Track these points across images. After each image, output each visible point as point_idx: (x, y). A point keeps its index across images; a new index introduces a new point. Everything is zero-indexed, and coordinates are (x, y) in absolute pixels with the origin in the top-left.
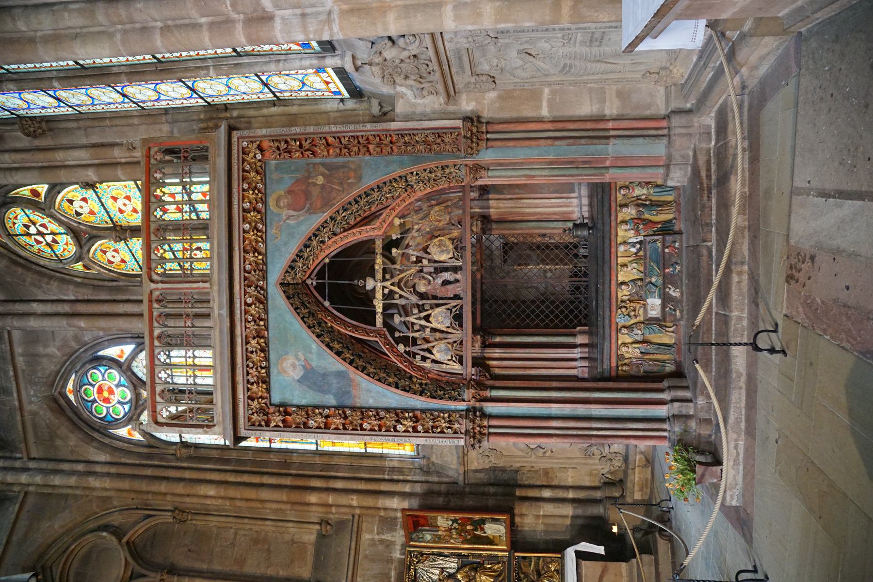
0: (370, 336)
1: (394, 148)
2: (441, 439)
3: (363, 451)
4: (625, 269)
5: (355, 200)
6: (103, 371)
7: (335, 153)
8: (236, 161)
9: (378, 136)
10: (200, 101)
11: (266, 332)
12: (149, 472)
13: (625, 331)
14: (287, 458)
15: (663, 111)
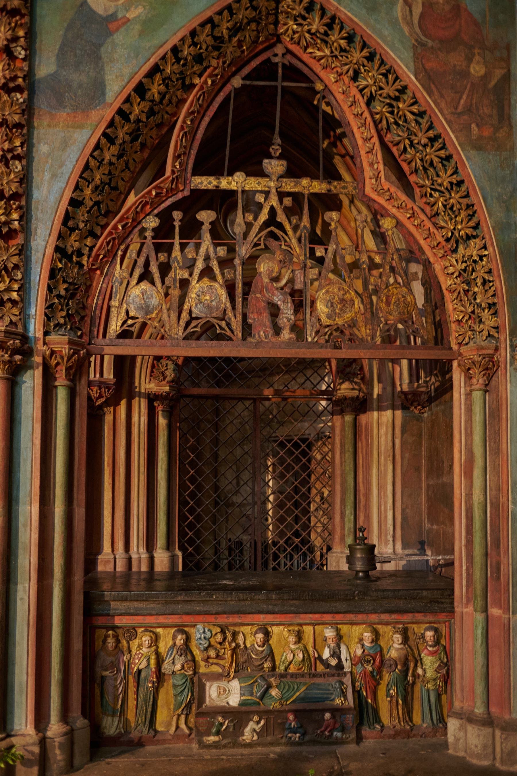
0: (174, 161)
4: (292, 639)
13: (180, 640)
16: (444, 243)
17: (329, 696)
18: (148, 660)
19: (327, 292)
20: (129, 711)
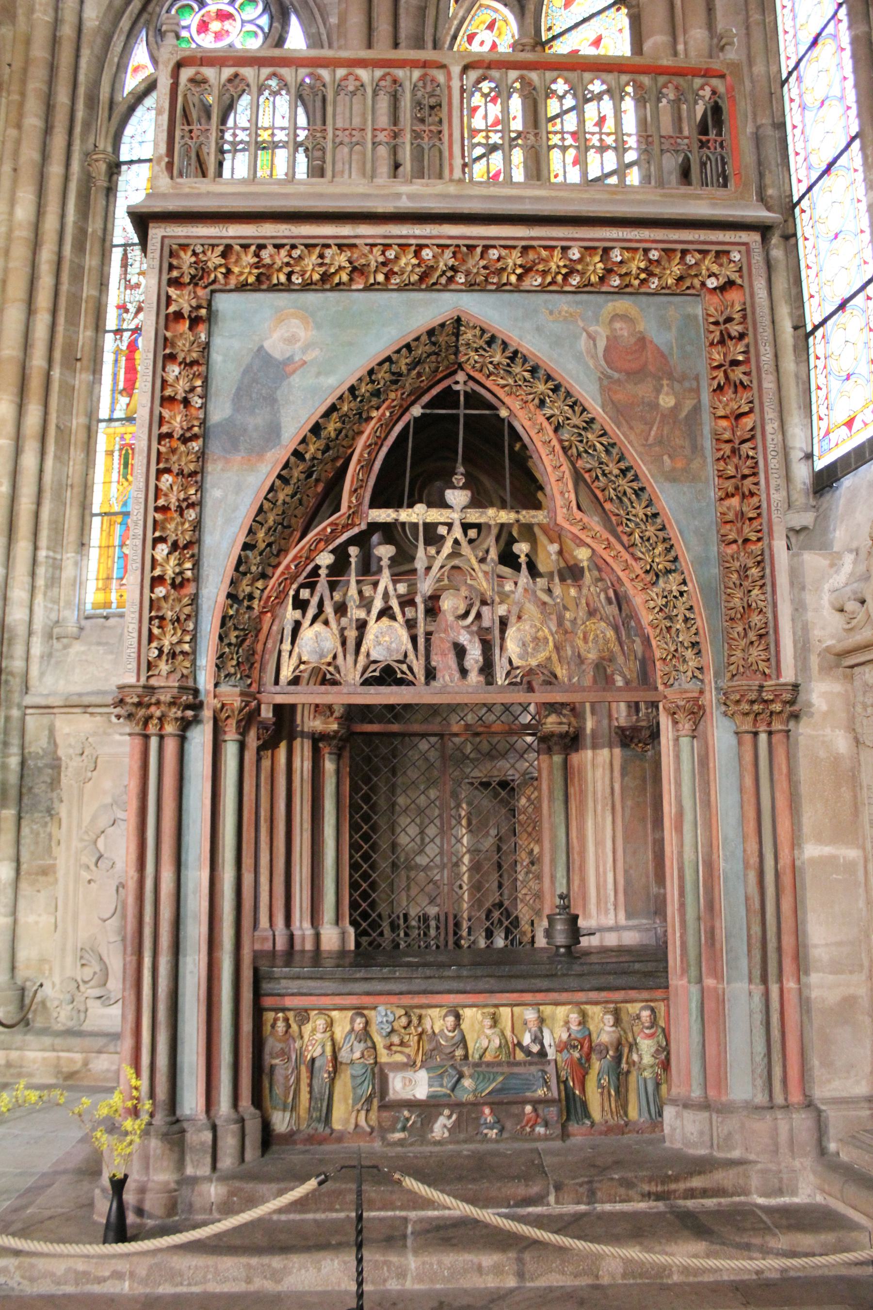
1: (734, 546)
2: (136, 635)
3: (96, 509)
4: (488, 1022)
5: (629, 469)
6: (258, 22)
7: (720, 430)
8: (702, 238)
9: (759, 515)
10: (803, 188)
11: (361, 287)
12: (62, 97)
13: (359, 1023)
14: (85, 361)
15: (820, 1093)
16: (643, 576)
18: (323, 1046)
19: (519, 629)
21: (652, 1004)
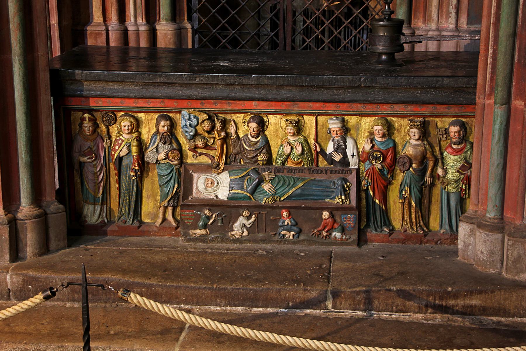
4: (291, 130)
13: (163, 127)
17: (330, 194)
18: (129, 147)
20: (112, 200)
21: (463, 120)
